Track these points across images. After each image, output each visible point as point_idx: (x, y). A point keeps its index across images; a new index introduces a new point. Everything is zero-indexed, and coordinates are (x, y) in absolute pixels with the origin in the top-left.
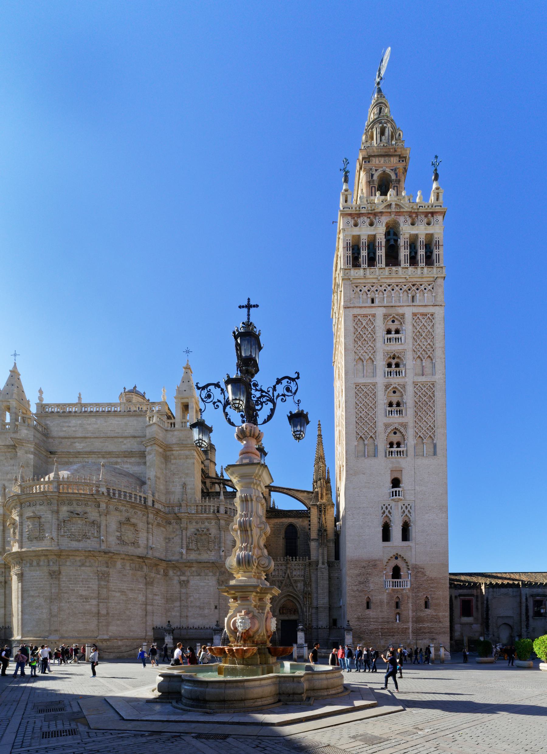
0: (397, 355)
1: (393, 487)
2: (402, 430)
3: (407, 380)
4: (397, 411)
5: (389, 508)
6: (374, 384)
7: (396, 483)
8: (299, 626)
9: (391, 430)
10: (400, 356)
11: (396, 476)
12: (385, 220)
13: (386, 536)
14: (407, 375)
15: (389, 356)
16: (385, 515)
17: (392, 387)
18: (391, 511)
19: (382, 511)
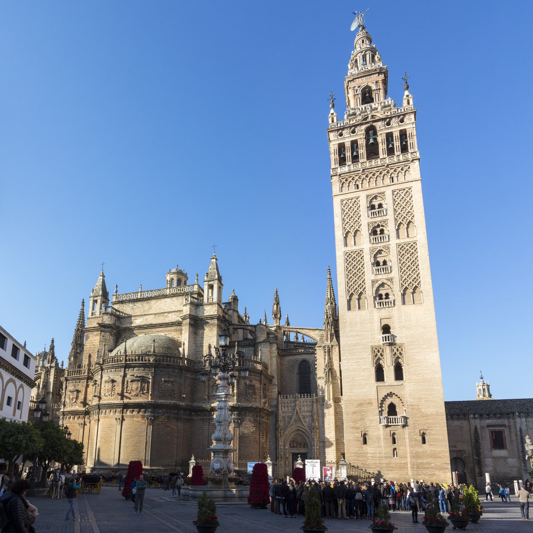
0: (381, 225)
1: (383, 333)
2: (389, 283)
3: (390, 243)
4: (383, 269)
5: (381, 350)
6: (361, 250)
7: (386, 329)
8: (298, 460)
9: (379, 285)
10: (383, 224)
11: (386, 323)
12: (364, 127)
13: (380, 375)
14: (391, 239)
15: (374, 226)
16: (377, 357)
17: (378, 250)
18: (383, 354)
19: (375, 354)
